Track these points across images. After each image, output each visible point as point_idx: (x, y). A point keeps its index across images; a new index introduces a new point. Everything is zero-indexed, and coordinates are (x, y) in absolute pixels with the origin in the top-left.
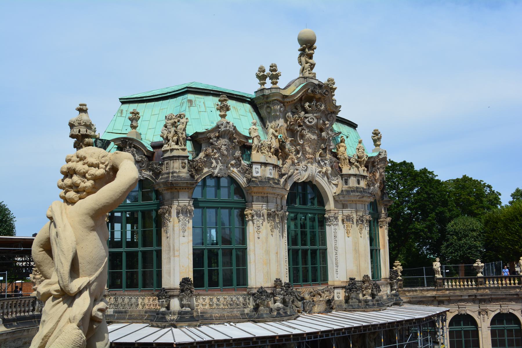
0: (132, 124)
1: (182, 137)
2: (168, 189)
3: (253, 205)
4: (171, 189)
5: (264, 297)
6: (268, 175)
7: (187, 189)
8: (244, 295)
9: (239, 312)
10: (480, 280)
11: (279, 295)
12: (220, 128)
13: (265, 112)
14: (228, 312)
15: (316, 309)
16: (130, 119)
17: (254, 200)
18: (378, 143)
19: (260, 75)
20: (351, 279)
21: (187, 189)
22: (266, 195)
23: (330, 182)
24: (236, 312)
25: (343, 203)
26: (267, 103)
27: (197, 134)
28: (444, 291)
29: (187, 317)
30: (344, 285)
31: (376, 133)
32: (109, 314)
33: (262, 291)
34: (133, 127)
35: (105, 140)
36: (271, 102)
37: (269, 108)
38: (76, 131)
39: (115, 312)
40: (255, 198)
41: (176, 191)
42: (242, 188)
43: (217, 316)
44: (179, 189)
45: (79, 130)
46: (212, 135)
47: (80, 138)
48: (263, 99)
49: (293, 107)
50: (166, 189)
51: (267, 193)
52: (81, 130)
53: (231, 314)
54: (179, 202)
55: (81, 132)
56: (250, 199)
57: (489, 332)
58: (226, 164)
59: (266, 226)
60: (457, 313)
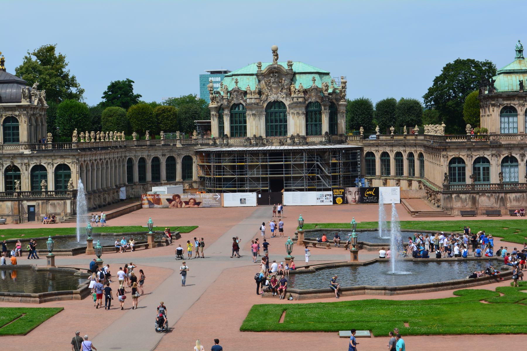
6: (253, 102)
15: (274, 144)
23: (286, 100)
24: (242, 144)
58: (237, 99)
59: (252, 118)
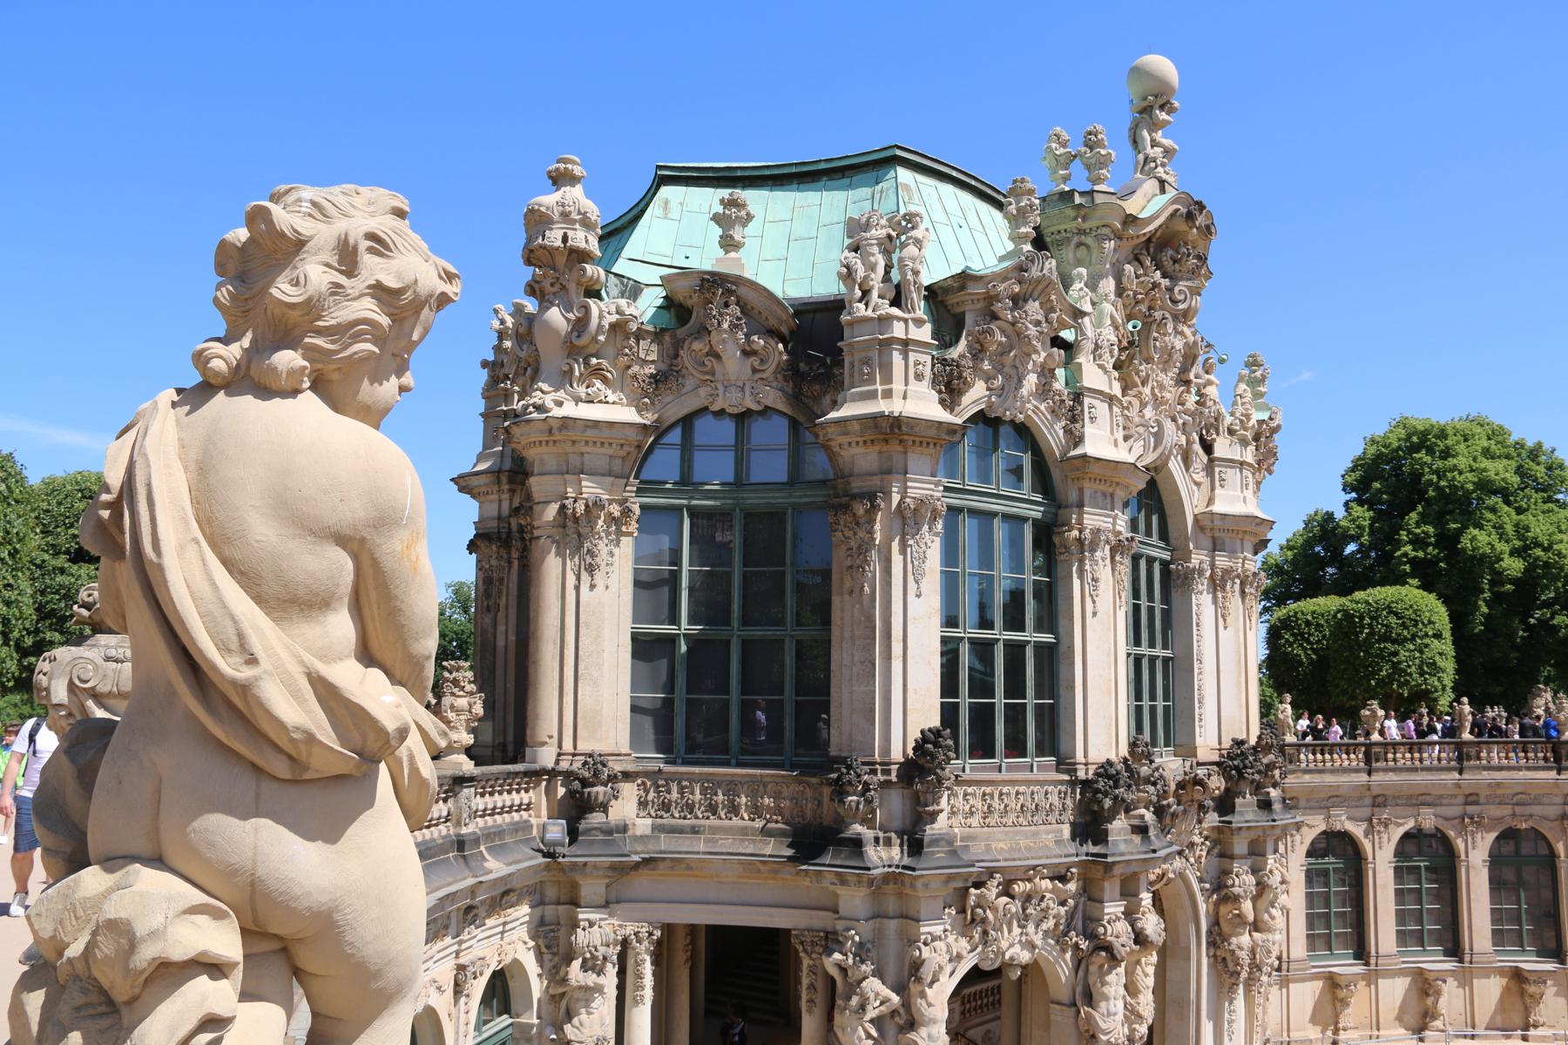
0: (731, 237)
1: (915, 283)
2: (872, 441)
3: (1085, 516)
4: (886, 441)
5: (1122, 790)
7: (931, 446)
8: (1061, 782)
9: (1050, 836)
10: (1376, 749)
11: (1145, 784)
12: (1026, 271)
13: (1071, 255)
14: (1027, 838)
16: (717, 219)
17: (1086, 501)
18: (1261, 389)
19: (1058, 153)
20: (1239, 743)
21: (931, 446)
22: (1111, 490)
25: (1217, 534)
26: (1082, 232)
27: (964, 279)
28: (1299, 774)
29: (938, 852)
30: (1216, 758)
31: (1253, 363)
32: (639, 832)
33: (1105, 770)
34: (728, 244)
35: (629, 279)
36: (1091, 229)
37: (1082, 247)
38: (554, 237)
39: (654, 828)
40: (1087, 494)
41: (900, 448)
42: (1050, 461)
43: (1001, 848)
44: (911, 443)
45: (565, 234)
46: (1001, 287)
47: (561, 261)
48: (1075, 219)
49: (1131, 257)
50: (865, 442)
51: (1117, 484)
52: (570, 233)
53: (1035, 843)
54: (909, 484)
55: (570, 243)
56: (1073, 497)
57: (1391, 872)
60: (1323, 827)
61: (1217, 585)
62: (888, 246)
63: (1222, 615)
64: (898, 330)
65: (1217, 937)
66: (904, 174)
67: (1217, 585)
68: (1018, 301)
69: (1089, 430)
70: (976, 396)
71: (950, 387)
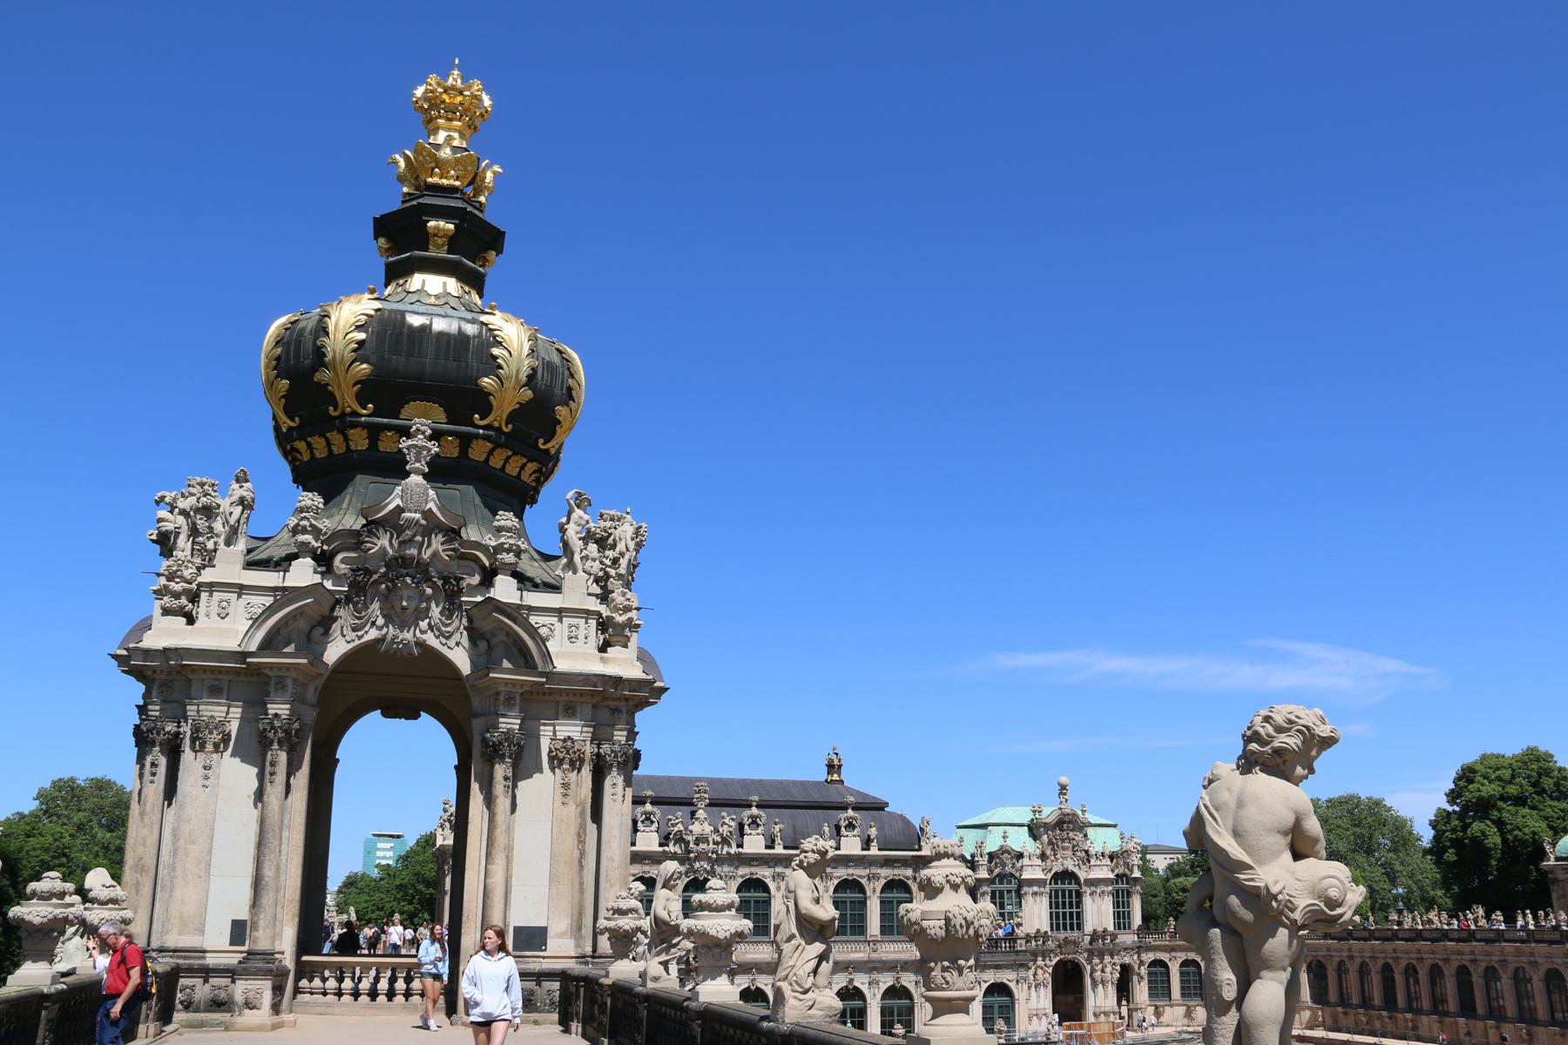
61: (1091, 894)
62: (980, 847)
63: (1094, 901)
64: (980, 863)
65: (1091, 974)
66: (990, 828)
67: (1091, 894)
68: (1002, 854)
69: (1024, 873)
70: (997, 871)
71: (990, 871)
